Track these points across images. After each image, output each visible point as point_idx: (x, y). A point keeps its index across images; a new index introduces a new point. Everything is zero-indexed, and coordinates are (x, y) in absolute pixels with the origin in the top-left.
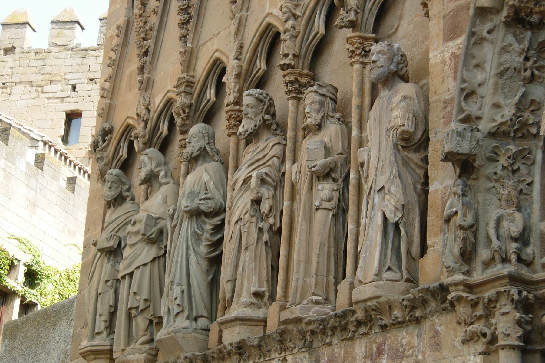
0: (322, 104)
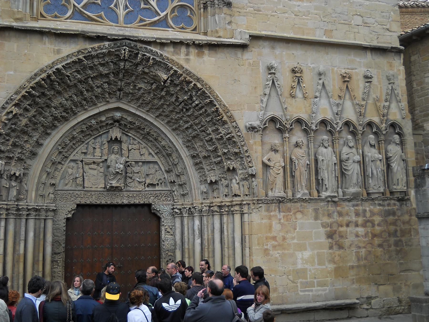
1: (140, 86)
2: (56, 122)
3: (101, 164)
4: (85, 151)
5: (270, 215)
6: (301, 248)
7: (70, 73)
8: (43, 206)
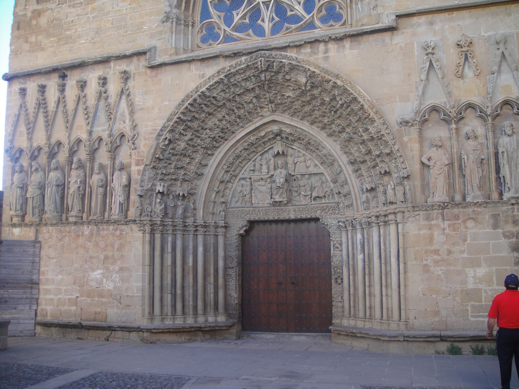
1: (287, 94)
2: (215, 143)
3: (268, 180)
4: (252, 168)
5: (431, 225)
6: (475, 263)
7: (217, 94)
8: (212, 223)
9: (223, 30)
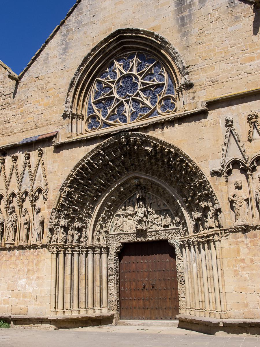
0: (25, 211)
5: (238, 241)
9: (101, 120)
